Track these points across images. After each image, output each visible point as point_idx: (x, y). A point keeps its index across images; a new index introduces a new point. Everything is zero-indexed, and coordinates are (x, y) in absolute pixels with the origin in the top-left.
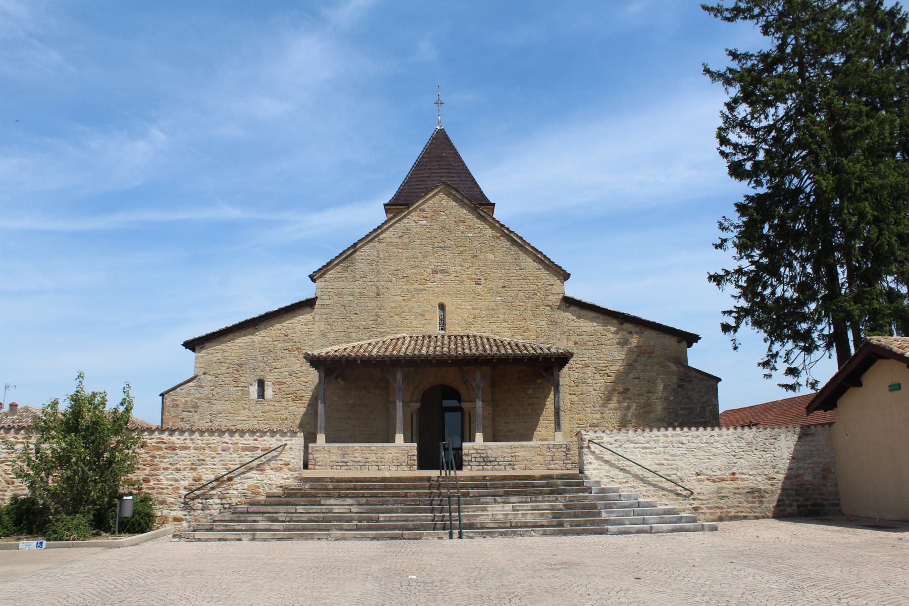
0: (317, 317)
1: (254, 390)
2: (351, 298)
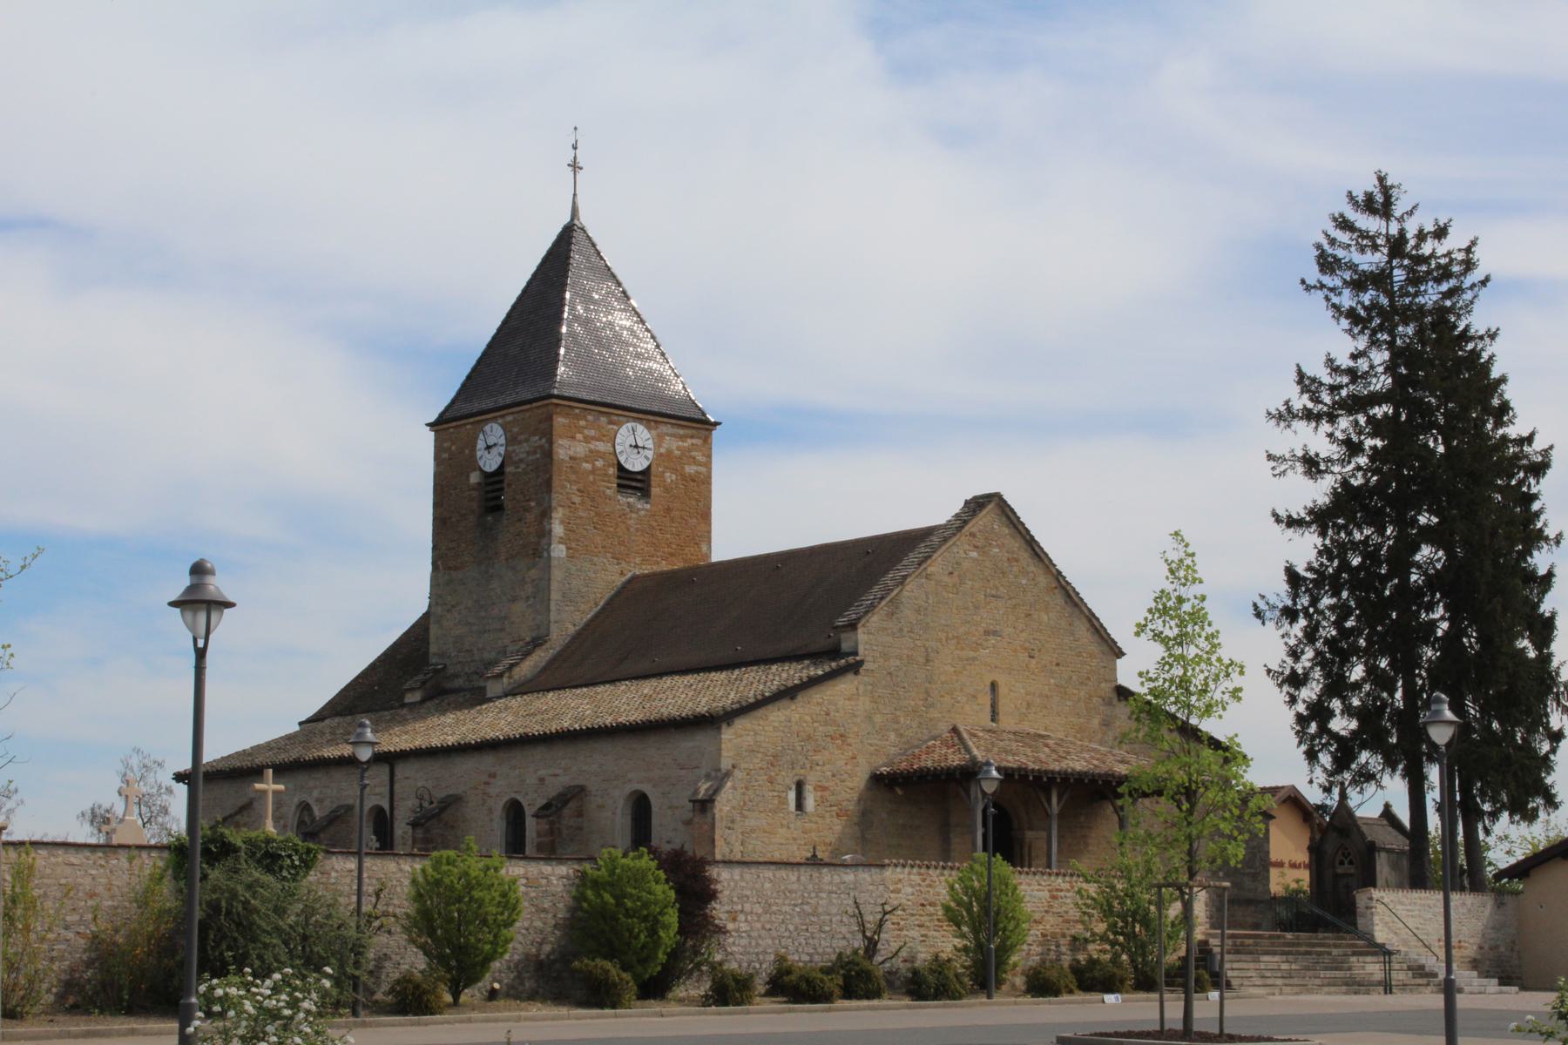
0: (861, 688)
1: (792, 795)
2: (898, 663)
